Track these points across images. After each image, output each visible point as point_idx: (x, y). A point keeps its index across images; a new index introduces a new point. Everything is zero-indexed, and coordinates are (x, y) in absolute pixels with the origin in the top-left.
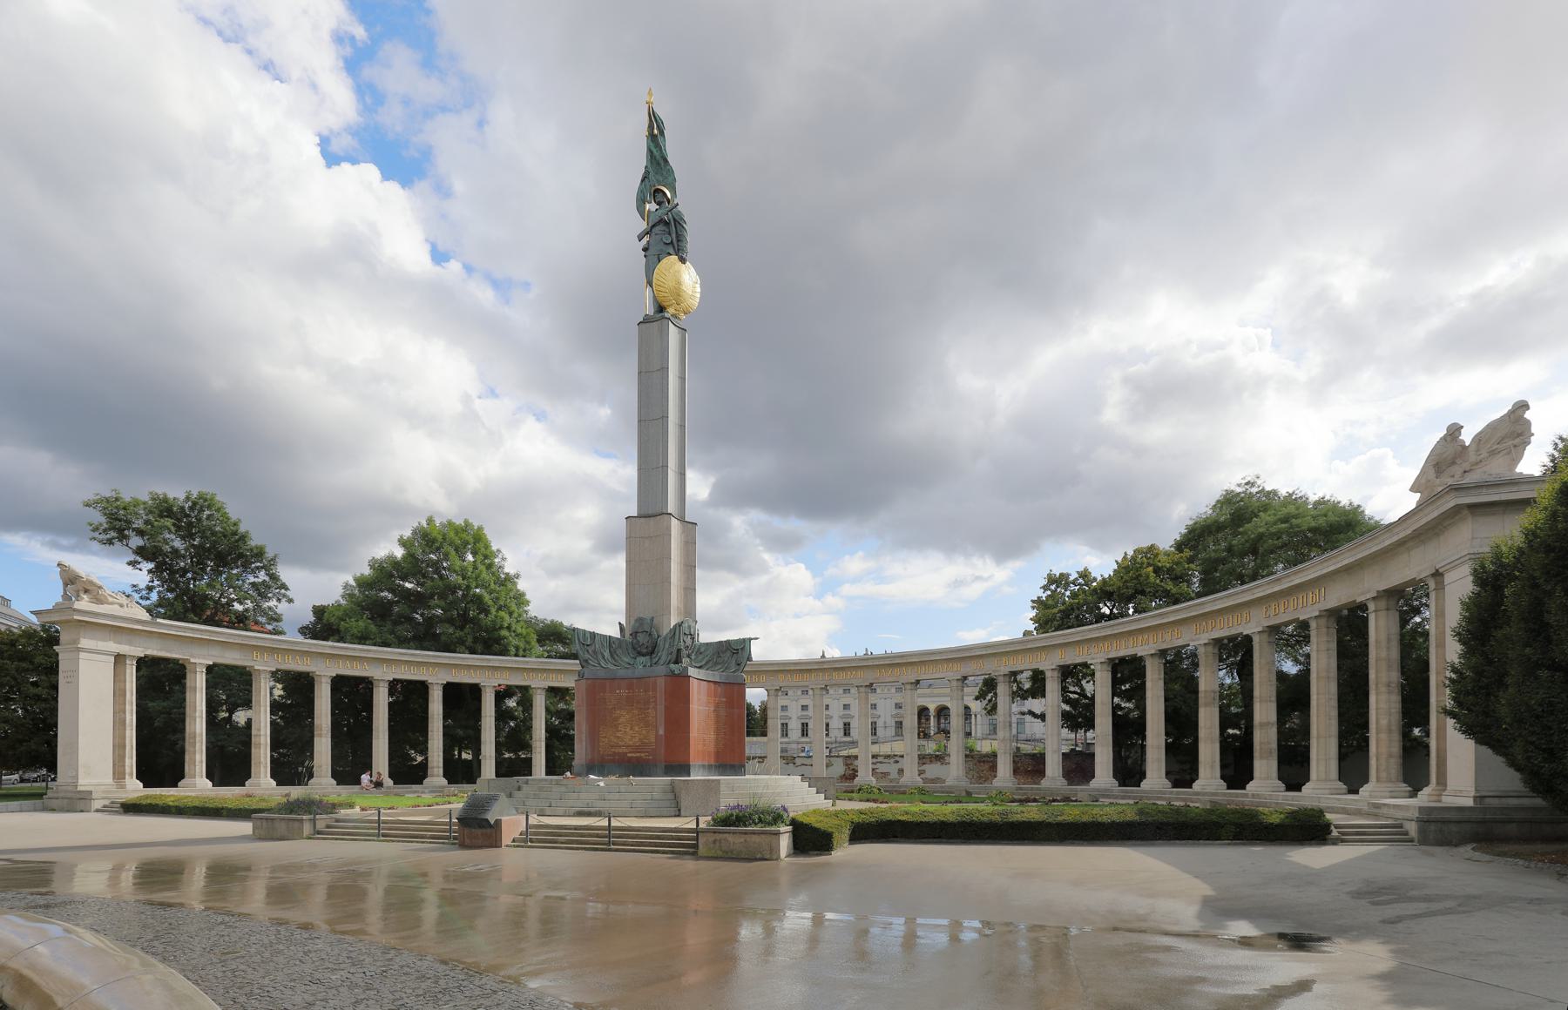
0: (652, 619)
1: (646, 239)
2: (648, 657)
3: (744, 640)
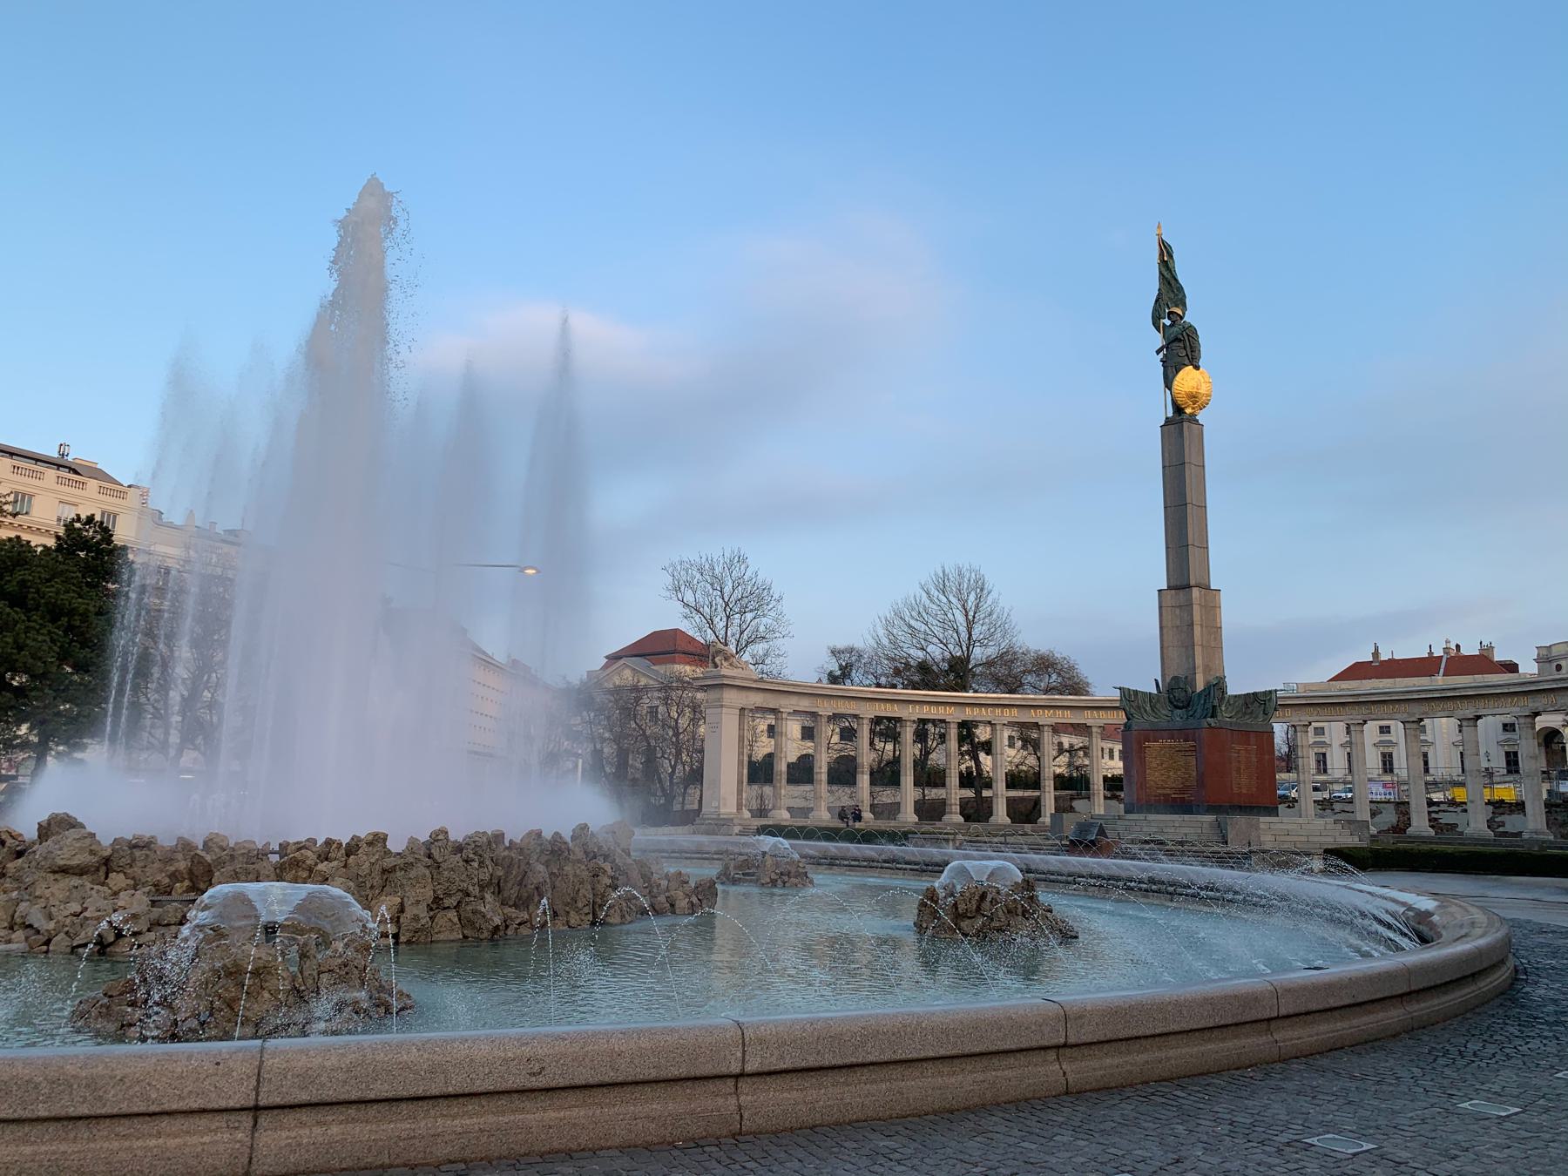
0: (1186, 677)
1: (1161, 355)
2: (1184, 710)
3: (1270, 692)
